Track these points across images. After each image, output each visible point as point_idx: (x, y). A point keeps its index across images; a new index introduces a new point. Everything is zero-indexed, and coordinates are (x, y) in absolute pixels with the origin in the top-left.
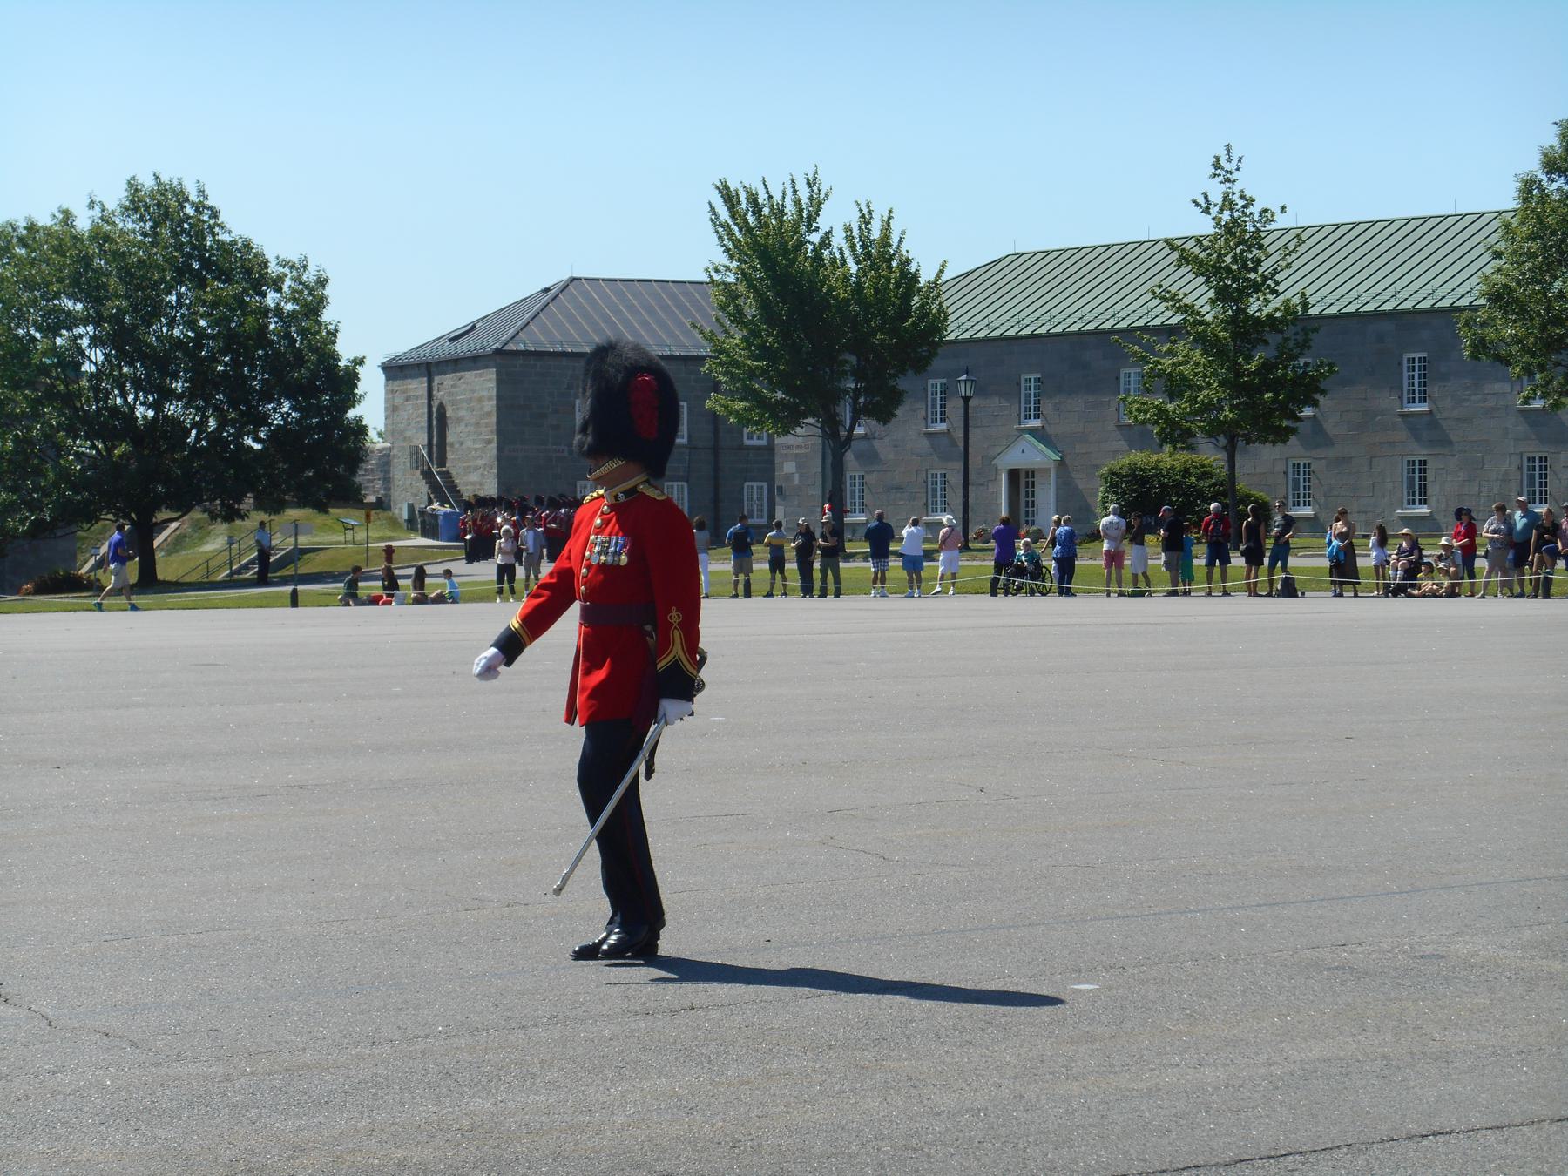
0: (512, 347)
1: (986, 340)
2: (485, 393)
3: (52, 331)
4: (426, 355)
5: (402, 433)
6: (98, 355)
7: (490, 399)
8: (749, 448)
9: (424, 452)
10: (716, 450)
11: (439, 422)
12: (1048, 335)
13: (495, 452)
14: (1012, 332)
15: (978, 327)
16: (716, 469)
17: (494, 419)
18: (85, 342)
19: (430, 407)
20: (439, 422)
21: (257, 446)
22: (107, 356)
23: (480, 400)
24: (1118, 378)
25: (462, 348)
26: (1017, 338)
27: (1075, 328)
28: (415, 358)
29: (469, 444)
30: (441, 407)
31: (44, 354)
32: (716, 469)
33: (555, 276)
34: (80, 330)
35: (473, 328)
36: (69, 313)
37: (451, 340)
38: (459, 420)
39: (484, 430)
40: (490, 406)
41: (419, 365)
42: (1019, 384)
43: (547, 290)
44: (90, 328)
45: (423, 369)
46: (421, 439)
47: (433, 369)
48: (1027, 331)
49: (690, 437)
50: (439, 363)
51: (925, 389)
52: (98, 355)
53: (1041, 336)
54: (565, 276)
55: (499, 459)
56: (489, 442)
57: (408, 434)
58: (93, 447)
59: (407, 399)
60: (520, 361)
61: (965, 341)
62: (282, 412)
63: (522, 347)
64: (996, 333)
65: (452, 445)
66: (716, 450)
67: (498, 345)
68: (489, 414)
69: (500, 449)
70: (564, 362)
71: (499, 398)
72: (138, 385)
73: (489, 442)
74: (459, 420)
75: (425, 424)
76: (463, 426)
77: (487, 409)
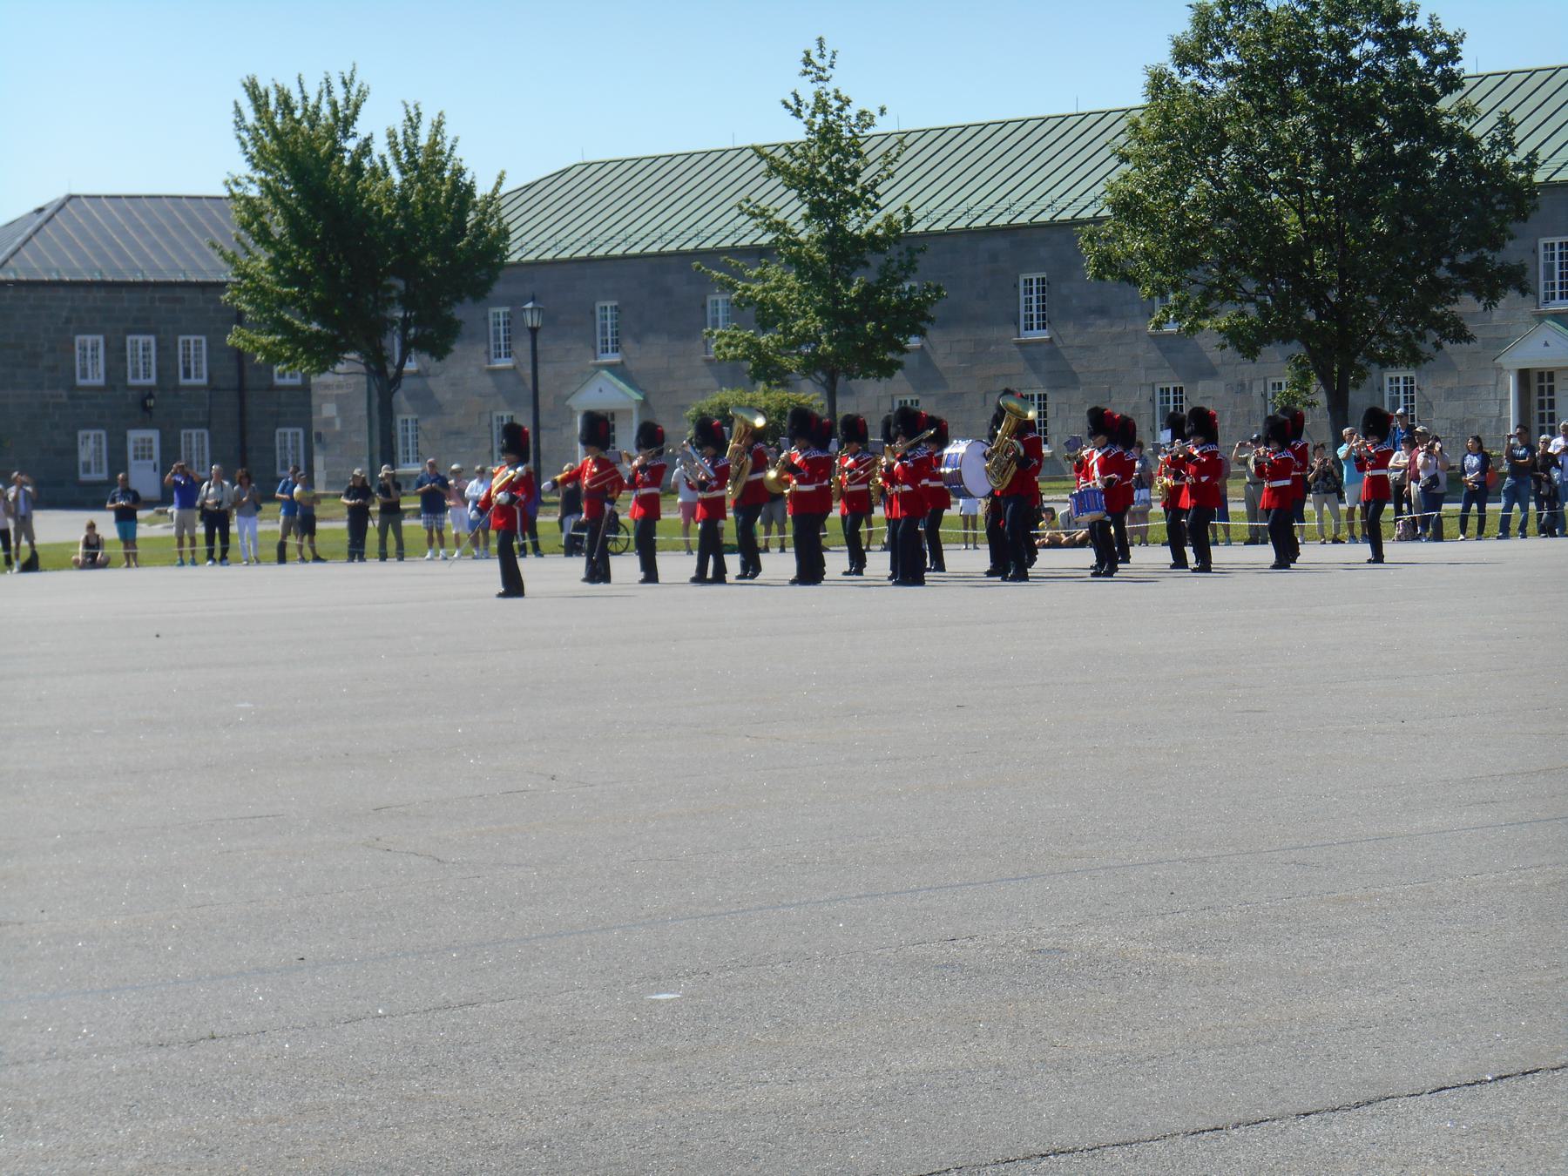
1: (554, 262)
10: (241, 391)
14: (583, 253)
16: (242, 414)
24: (704, 307)
26: (589, 260)
27: (654, 249)
32: (242, 414)
42: (593, 313)
48: (601, 252)
49: (210, 378)
51: (486, 319)
53: (616, 258)
61: (529, 264)
64: (566, 255)
66: (241, 391)
70: (62, 292)
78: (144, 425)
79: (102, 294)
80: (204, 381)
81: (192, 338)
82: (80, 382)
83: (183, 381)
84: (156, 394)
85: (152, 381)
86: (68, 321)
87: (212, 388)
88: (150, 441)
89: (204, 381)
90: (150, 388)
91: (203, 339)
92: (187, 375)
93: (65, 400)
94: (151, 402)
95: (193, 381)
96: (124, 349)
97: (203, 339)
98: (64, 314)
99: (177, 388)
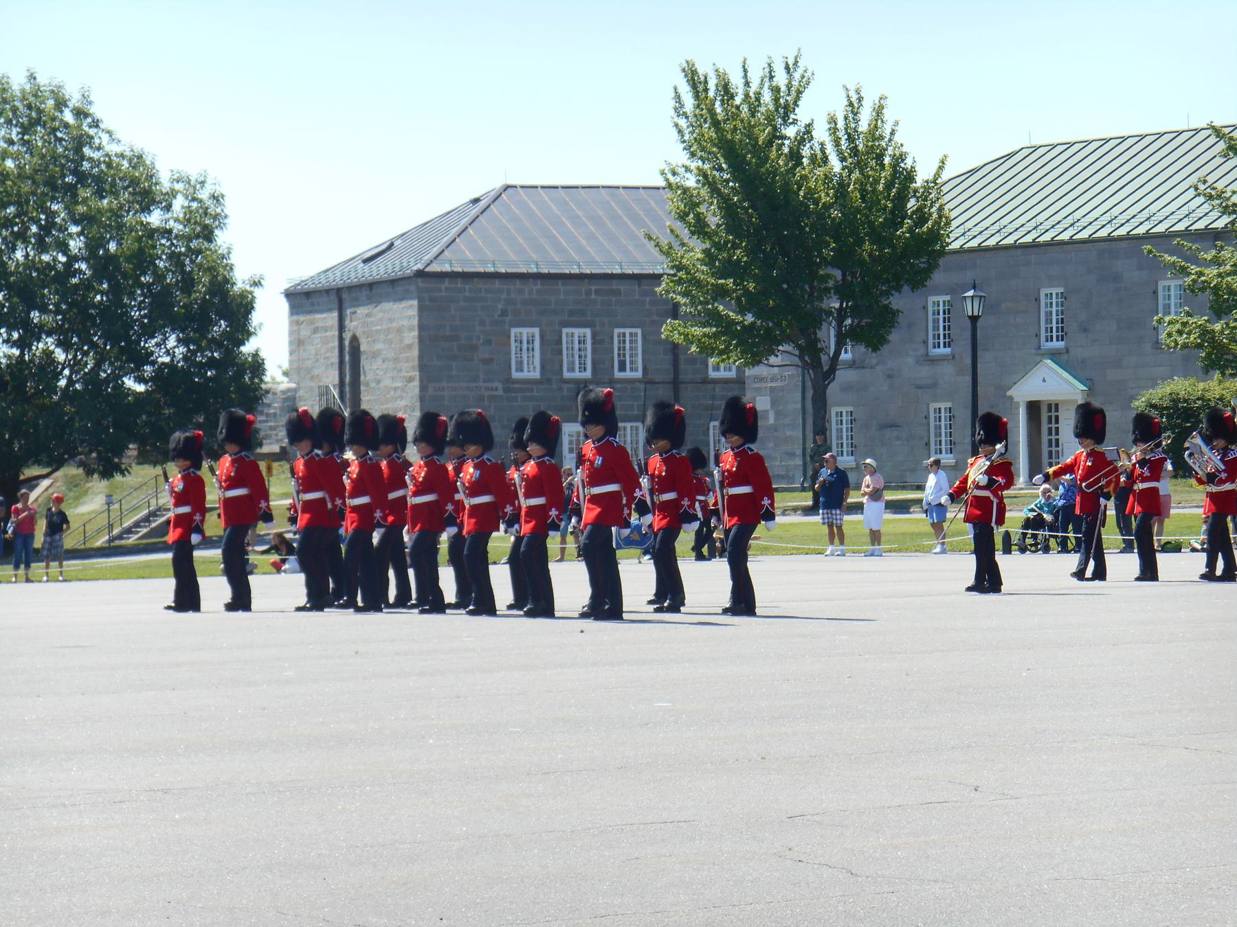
1: (998, 248)
2: (405, 323)
4: (336, 280)
5: (309, 370)
7: (411, 329)
8: (715, 381)
9: (336, 394)
11: (351, 358)
12: (1071, 242)
13: (417, 391)
14: (1028, 239)
15: (987, 234)
17: (415, 353)
19: (341, 339)
20: (351, 358)
21: (140, 388)
23: (399, 330)
24: (1155, 292)
25: (379, 270)
26: (1034, 245)
27: (1103, 233)
28: (324, 283)
29: (387, 382)
35: (392, 244)
37: (366, 261)
38: (375, 355)
40: (412, 337)
41: (328, 291)
42: (1037, 300)
43: (476, 201)
45: (333, 297)
47: (345, 296)
48: (1047, 237)
49: (645, 369)
50: (351, 288)
51: (925, 308)
53: (1062, 243)
54: (498, 184)
56: (411, 380)
57: (316, 372)
59: (316, 331)
60: (446, 283)
61: (972, 251)
62: (169, 348)
63: (447, 268)
64: (1010, 241)
65: (367, 384)
67: (420, 266)
68: (410, 347)
69: (423, 388)
70: (497, 284)
71: (421, 327)
73: (411, 380)
74: (375, 355)
75: (336, 360)
76: (379, 362)
77: (407, 341)
79: (537, 286)
81: (627, 331)
82: (516, 375)
83: (618, 375)
85: (588, 374)
86: (504, 313)
87: (647, 381)
91: (639, 331)
92: (622, 368)
93: (500, 392)
95: (628, 374)
96: (560, 342)
97: (639, 331)
98: (500, 306)
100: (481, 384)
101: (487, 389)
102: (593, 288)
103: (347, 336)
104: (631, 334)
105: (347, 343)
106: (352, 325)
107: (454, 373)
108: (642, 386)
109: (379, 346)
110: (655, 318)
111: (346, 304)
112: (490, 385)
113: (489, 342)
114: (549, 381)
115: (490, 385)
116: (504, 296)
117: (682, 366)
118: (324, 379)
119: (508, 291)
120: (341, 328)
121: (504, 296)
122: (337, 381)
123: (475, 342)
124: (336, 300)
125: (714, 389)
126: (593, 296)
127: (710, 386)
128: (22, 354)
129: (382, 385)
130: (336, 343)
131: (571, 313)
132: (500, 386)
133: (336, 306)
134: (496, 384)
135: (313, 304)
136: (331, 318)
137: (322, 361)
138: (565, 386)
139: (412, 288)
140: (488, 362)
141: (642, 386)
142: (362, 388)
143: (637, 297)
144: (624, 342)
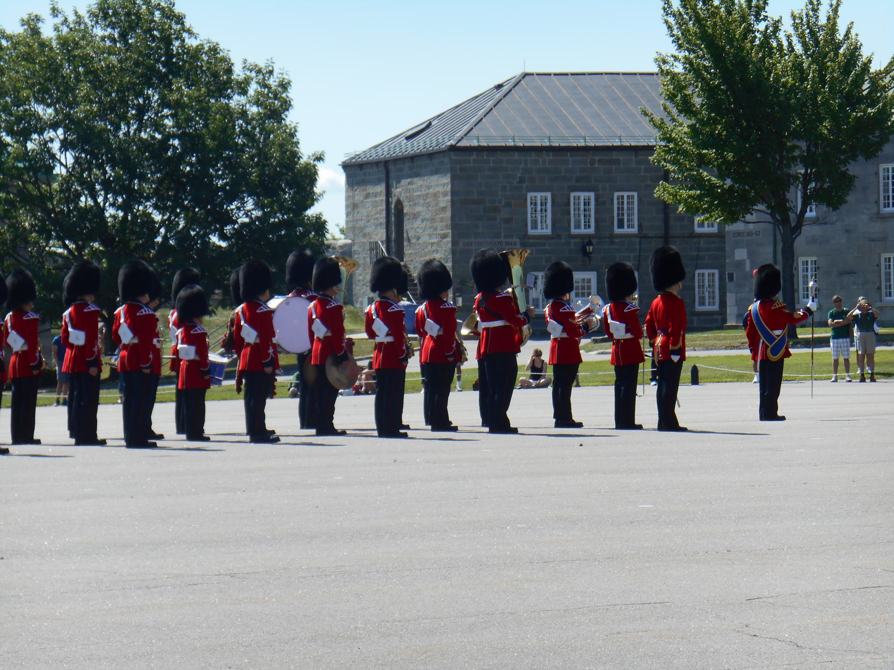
0: (464, 143)
2: (440, 189)
3: (24, 135)
4: (384, 153)
5: (362, 229)
6: (69, 158)
7: (445, 194)
11: (396, 217)
13: (450, 245)
17: (448, 214)
18: (55, 146)
19: (388, 203)
20: (396, 217)
21: (224, 244)
22: (77, 160)
23: (435, 195)
28: (374, 156)
29: (425, 239)
30: (399, 203)
31: (17, 159)
33: (507, 73)
34: (49, 134)
35: (430, 124)
36: (39, 119)
37: (408, 138)
38: (415, 216)
39: (439, 225)
40: (445, 201)
41: (376, 163)
43: (499, 87)
44: (60, 131)
46: (379, 235)
47: (391, 167)
49: (640, 226)
50: (397, 160)
51: (877, 174)
52: (69, 158)
54: (517, 72)
55: (453, 252)
56: (444, 236)
57: (367, 230)
58: (65, 247)
59: (367, 196)
60: (474, 156)
62: (246, 211)
63: (475, 143)
65: (409, 240)
67: (452, 142)
68: (444, 209)
69: (454, 243)
70: (516, 156)
71: (453, 193)
72: (107, 186)
73: (444, 236)
74: (415, 216)
75: (383, 220)
76: (419, 222)
77: (442, 204)
78: (584, 269)
79: (551, 156)
80: (635, 230)
81: (625, 194)
82: (531, 232)
83: (617, 231)
84: (594, 241)
85: (591, 231)
86: (522, 180)
87: (642, 236)
88: (589, 281)
89: (635, 230)
90: (589, 236)
91: (635, 194)
92: (621, 225)
94: (590, 249)
95: (626, 230)
96: (568, 204)
97: (635, 194)
98: (519, 175)
99: (612, 236)
100: (502, 240)
101: (508, 243)
102: (597, 158)
103: (393, 200)
104: (628, 197)
105: (393, 206)
106: (397, 191)
107: (480, 230)
108: (638, 240)
109: (418, 209)
110: (649, 183)
111: (393, 175)
112: (510, 240)
113: (508, 205)
114: (559, 237)
115: (510, 240)
116: (522, 166)
117: (672, 223)
118: (374, 236)
119: (526, 161)
120: (388, 194)
121: (522, 166)
122: (384, 238)
123: (497, 204)
124: (384, 171)
125: (699, 243)
126: (597, 165)
127: (695, 240)
128: (125, 216)
129: (421, 241)
130: (384, 207)
131: (579, 180)
132: (518, 241)
133: (384, 176)
134: (515, 240)
135: (365, 174)
136: (381, 188)
137: (372, 221)
138: (572, 241)
139: (447, 160)
140: (508, 221)
141: (638, 240)
142: (405, 243)
143: (634, 165)
144: (623, 203)
